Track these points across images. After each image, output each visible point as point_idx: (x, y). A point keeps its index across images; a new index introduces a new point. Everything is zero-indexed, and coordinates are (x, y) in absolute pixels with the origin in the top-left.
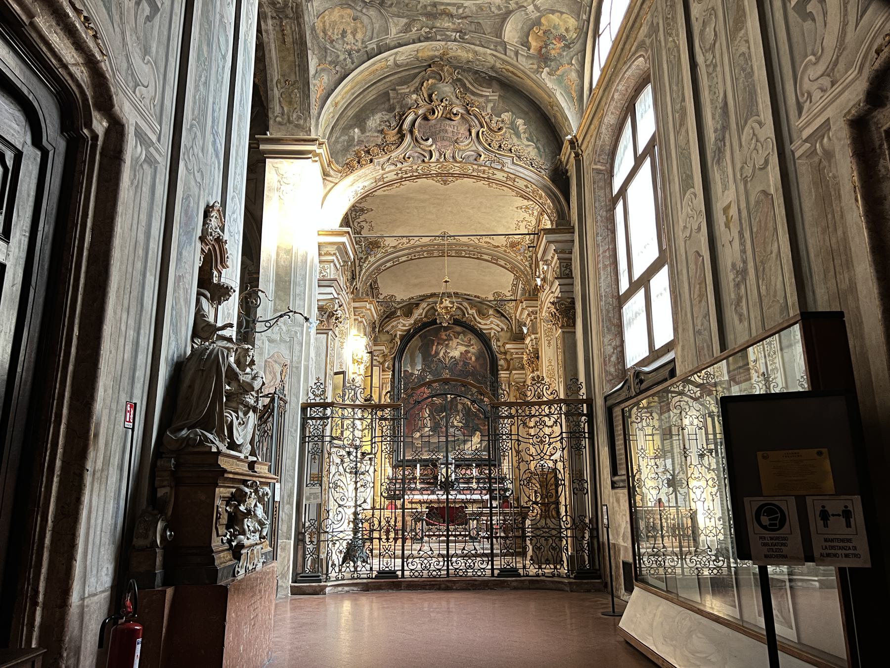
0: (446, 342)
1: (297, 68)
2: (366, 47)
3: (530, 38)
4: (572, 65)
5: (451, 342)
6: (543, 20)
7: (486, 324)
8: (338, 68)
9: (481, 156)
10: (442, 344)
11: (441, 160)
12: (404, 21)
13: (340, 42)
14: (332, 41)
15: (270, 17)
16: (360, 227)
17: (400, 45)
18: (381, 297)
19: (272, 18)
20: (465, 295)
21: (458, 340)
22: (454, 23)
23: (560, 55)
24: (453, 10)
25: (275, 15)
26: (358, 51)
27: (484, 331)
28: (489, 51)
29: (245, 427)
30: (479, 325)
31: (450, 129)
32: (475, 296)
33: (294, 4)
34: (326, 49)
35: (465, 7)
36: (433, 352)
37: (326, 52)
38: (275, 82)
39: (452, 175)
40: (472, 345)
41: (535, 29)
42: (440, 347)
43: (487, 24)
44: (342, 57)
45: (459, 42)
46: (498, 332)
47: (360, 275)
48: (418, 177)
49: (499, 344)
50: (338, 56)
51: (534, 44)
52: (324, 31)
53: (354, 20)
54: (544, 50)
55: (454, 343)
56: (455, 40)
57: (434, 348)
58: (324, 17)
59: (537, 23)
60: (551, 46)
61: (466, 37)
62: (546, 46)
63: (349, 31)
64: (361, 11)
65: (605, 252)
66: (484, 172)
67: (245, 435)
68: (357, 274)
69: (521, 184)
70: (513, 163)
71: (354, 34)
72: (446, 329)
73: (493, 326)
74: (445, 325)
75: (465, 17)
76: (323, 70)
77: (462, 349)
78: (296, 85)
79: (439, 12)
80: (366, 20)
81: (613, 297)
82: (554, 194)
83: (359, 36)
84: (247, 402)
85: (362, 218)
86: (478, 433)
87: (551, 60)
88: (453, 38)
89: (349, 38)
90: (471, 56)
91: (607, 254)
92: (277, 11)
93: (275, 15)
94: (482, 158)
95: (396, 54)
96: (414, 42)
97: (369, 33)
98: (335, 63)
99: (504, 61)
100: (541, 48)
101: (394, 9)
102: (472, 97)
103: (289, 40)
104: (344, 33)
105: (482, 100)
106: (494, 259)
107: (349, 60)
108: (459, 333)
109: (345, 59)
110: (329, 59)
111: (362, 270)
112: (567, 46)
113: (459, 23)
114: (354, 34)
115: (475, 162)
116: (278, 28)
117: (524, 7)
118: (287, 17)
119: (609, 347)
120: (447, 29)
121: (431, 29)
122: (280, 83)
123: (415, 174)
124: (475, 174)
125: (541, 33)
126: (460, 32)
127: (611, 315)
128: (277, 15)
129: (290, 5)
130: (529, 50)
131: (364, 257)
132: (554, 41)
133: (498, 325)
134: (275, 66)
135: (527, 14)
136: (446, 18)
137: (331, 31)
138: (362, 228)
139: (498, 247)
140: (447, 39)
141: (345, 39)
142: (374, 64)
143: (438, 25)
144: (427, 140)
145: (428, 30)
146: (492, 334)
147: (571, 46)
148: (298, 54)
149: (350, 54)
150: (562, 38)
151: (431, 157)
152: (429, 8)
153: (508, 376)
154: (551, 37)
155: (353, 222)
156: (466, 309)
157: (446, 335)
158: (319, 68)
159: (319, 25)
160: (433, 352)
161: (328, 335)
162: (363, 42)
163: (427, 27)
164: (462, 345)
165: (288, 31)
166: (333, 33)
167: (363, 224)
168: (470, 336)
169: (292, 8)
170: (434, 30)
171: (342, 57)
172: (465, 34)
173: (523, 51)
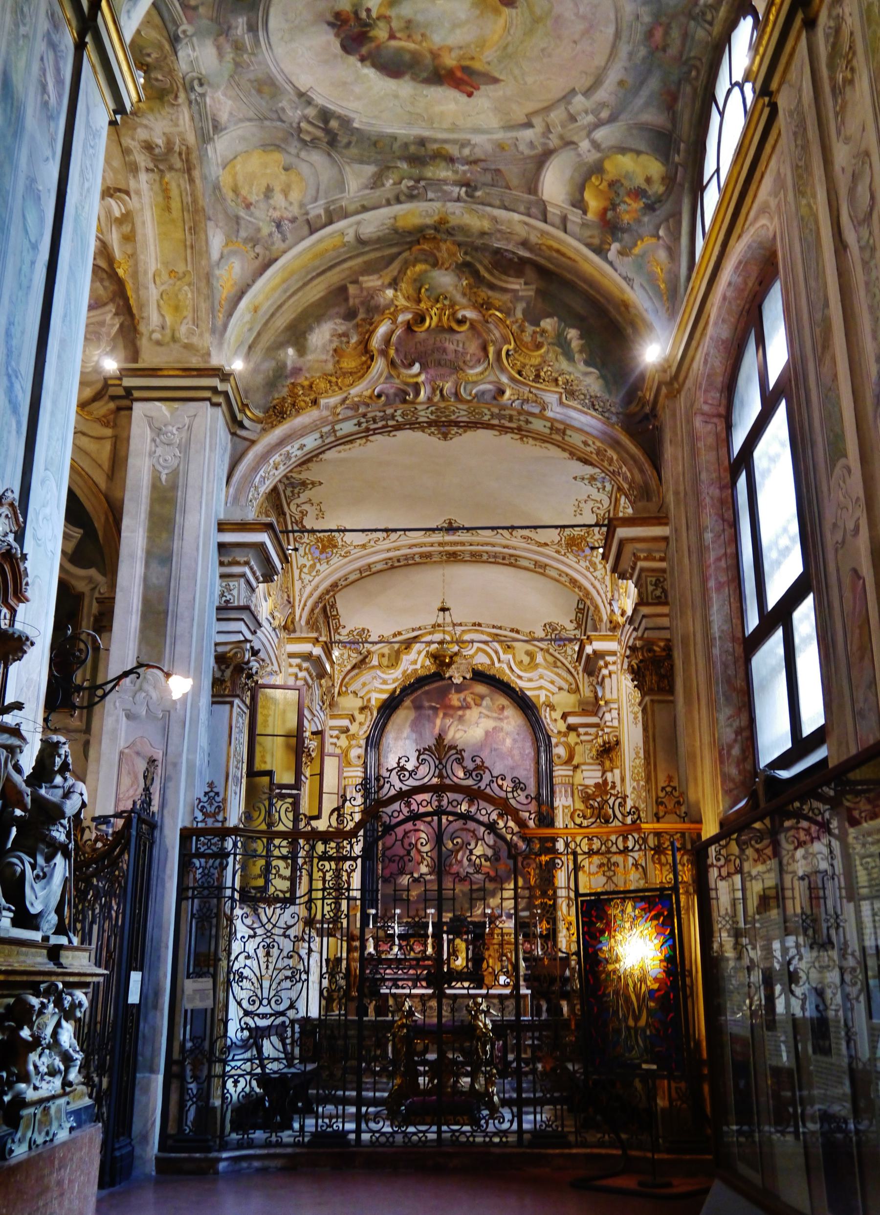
0: (460, 713)
1: (189, 251)
2: (307, 213)
3: (587, 195)
4: (659, 238)
5: (468, 712)
6: (608, 165)
7: (530, 680)
8: (258, 249)
9: (503, 392)
10: (452, 716)
11: (437, 398)
12: (370, 170)
13: (262, 205)
14: (248, 206)
15: (143, 169)
16: (301, 512)
17: (365, 209)
18: (344, 632)
19: (147, 170)
21: (480, 709)
22: (456, 172)
23: (639, 221)
24: (453, 150)
25: (151, 166)
26: (293, 220)
27: (528, 693)
28: (516, 217)
29: (49, 883)
30: (519, 682)
31: (451, 347)
32: (512, 630)
33: (184, 148)
34: (237, 219)
35: (474, 146)
37: (238, 223)
38: (150, 275)
39: (457, 424)
41: (593, 179)
42: (448, 721)
43: (513, 173)
44: (265, 231)
45: (465, 202)
46: (553, 694)
47: (301, 595)
48: (399, 427)
50: (259, 230)
51: (593, 203)
52: (235, 191)
53: (286, 169)
54: (610, 214)
55: (472, 714)
56: (458, 199)
58: (234, 167)
59: (598, 169)
60: (623, 207)
61: (478, 194)
62: (614, 206)
63: (277, 189)
64: (298, 156)
65: (719, 559)
66: (511, 419)
67: (47, 897)
68: (297, 593)
69: (576, 439)
70: (561, 403)
71: (286, 193)
72: (459, 688)
73: (543, 682)
75: (475, 162)
76: (234, 253)
78: (186, 279)
79: (430, 153)
80: (305, 169)
81: (734, 639)
82: (633, 457)
83: (295, 195)
84: (54, 838)
85: (304, 497)
87: (623, 231)
88: (455, 195)
89: (278, 199)
90: (486, 225)
91: (723, 564)
92: (156, 159)
93: (151, 166)
94: (508, 393)
95: (359, 223)
96: (389, 203)
97: (312, 192)
98: (254, 241)
99: (543, 233)
100: (605, 211)
101: (354, 151)
103: (175, 205)
104: (268, 192)
106: (540, 567)
107: (277, 236)
108: (482, 697)
109: (271, 235)
110: (243, 234)
111: (304, 587)
112: (650, 208)
113: (465, 172)
114: (286, 193)
115: (495, 402)
116: (156, 187)
117: (573, 143)
118: (171, 168)
119: (728, 730)
120: (445, 181)
121: (418, 181)
122: (160, 276)
123: (391, 423)
124: (495, 422)
125: (604, 186)
126: (467, 184)
127: (731, 672)
128: (156, 166)
129: (177, 149)
130: (585, 212)
131: (308, 564)
132: (627, 200)
133: (552, 682)
134: (152, 248)
135: (579, 155)
136: (443, 164)
137: (247, 188)
138: (304, 514)
139: (546, 544)
140: (447, 198)
141: (271, 202)
142: (320, 241)
143: (429, 174)
144: (411, 365)
145: (411, 183)
146: (542, 699)
147: (656, 206)
148: (190, 229)
149: (279, 226)
150: (638, 193)
151: (417, 394)
152: (412, 149)
153: (571, 773)
154: (622, 192)
155: (288, 505)
156: (496, 652)
157: (459, 700)
158: (225, 251)
159: (225, 179)
161: (232, 706)
162: (302, 205)
163: (410, 178)
164: (488, 717)
165: (174, 193)
166: (250, 193)
167: (306, 507)
169: (180, 154)
170: (422, 183)
171: (265, 231)
172: (476, 189)
173: (575, 216)
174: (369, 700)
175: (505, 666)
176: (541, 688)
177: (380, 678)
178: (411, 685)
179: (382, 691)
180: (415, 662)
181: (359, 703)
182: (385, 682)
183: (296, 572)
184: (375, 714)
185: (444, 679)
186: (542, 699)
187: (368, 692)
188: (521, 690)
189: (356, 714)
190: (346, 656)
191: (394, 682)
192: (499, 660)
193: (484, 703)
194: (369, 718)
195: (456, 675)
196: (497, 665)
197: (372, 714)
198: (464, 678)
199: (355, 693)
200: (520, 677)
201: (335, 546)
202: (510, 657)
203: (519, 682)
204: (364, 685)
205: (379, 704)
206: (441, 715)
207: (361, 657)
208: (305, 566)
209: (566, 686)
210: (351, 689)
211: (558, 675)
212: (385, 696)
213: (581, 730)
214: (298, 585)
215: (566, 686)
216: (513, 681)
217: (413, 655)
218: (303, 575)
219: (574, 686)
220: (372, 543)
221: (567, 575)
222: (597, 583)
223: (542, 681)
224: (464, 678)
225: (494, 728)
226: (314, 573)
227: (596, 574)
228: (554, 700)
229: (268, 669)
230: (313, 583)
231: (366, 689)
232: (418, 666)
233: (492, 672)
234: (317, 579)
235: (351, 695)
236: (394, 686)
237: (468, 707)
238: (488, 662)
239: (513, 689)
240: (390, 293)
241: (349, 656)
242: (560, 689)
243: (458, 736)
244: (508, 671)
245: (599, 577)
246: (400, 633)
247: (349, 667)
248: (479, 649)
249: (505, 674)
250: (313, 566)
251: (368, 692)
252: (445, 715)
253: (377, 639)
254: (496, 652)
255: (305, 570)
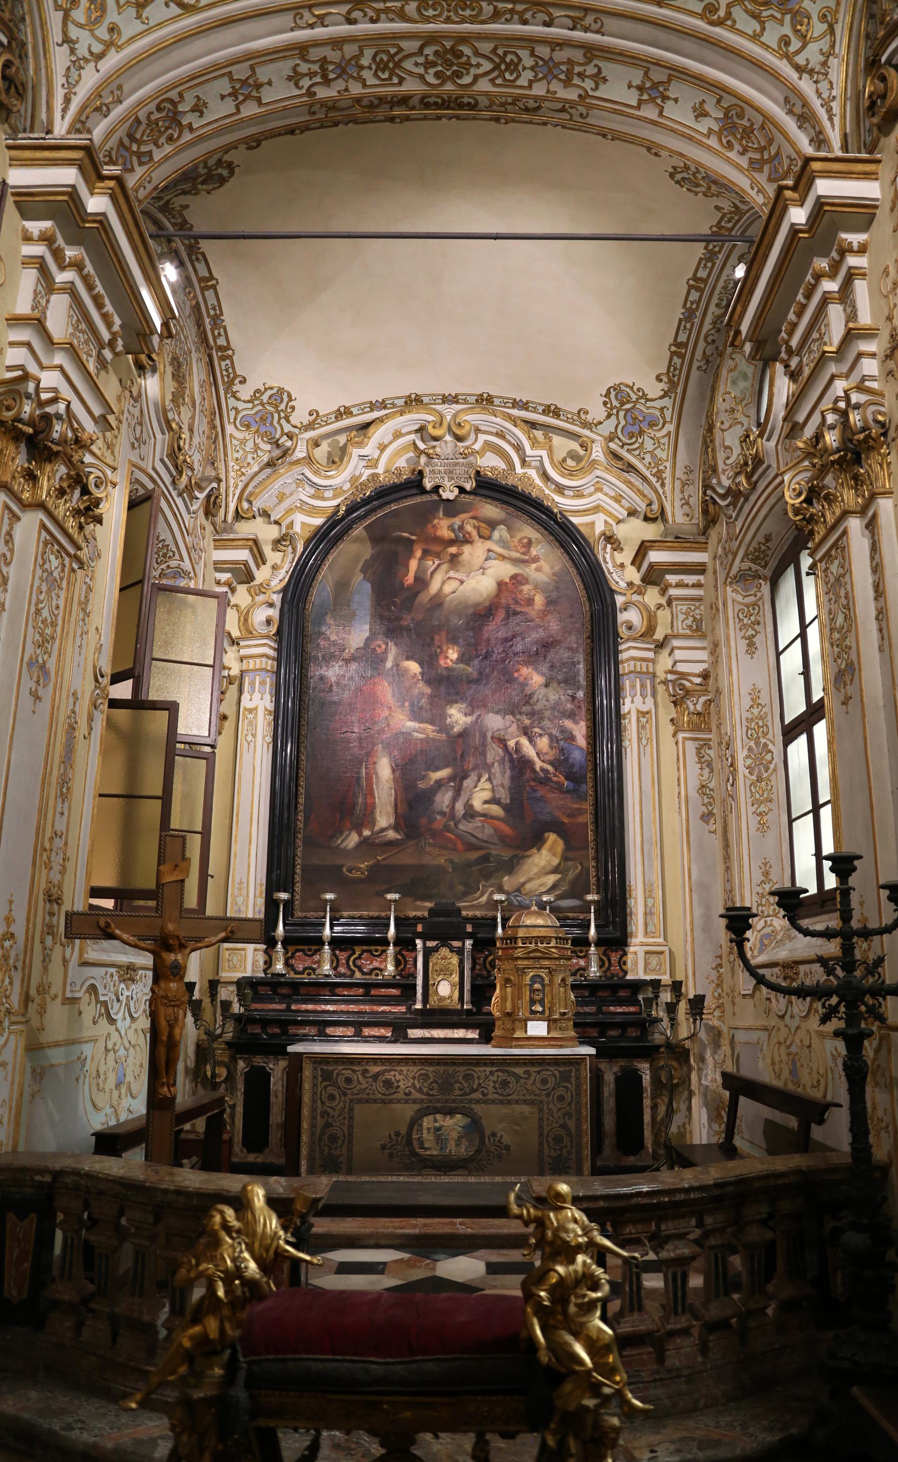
0: (453, 550)
5: (467, 549)
10: (438, 555)
18: (245, 392)
20: (515, 404)
21: (489, 544)
27: (575, 520)
32: (547, 411)
36: (410, 579)
40: (536, 560)
42: (431, 564)
49: (620, 558)
55: (474, 553)
57: (413, 564)
72: (451, 508)
74: (449, 493)
77: (505, 570)
86: (552, 837)
108: (493, 525)
156: (519, 448)
157: (451, 528)
160: (410, 579)
164: (503, 558)
168: (529, 531)
185: (423, 491)
192: (524, 463)
193: (496, 535)
195: (447, 484)
196: (519, 470)
198: (462, 490)
204: (281, 497)
206: (418, 554)
224: (462, 490)
225: (514, 577)
237: (468, 541)
239: (548, 512)
243: (448, 589)
252: (426, 553)
253: (306, 419)
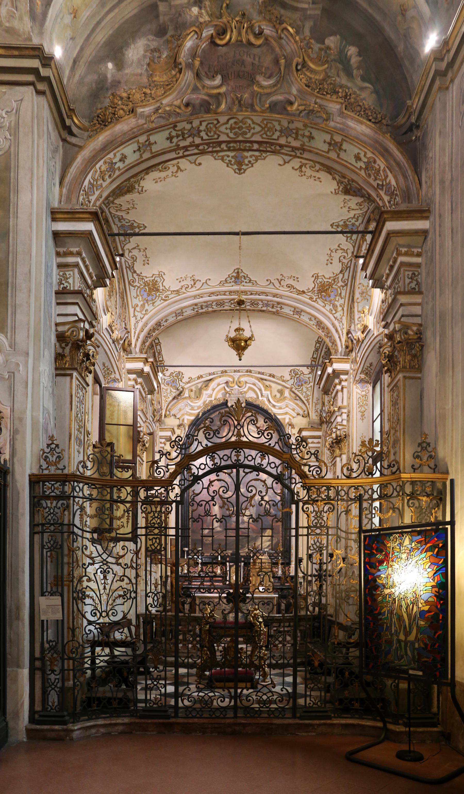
31: (249, 60)
102: (282, 11)
105: (297, 15)
144: (213, 78)
174: (183, 420)
175: (265, 399)
176: (286, 413)
177: (190, 405)
178: (209, 411)
179: (190, 414)
180: (210, 396)
181: (177, 422)
182: (192, 409)
183: (132, 310)
184: (187, 429)
186: (287, 421)
187: (183, 415)
188: (274, 415)
189: (176, 429)
190: (169, 391)
191: (198, 409)
194: (183, 432)
197: (185, 429)
199: (175, 416)
200: (274, 406)
201: (158, 290)
202: (269, 393)
203: (273, 409)
205: (189, 423)
207: (178, 392)
208: (137, 306)
209: (301, 412)
210: (172, 412)
211: (297, 404)
212: (192, 418)
213: (310, 440)
214: (133, 320)
215: (301, 412)
216: (270, 409)
217: (209, 391)
218: (136, 313)
219: (306, 413)
220: (183, 290)
221: (316, 318)
222: (336, 323)
223: (287, 409)
226: (144, 312)
227: (338, 315)
228: (294, 421)
229: (112, 376)
230: (144, 320)
231: (182, 413)
232: (213, 399)
233: (257, 403)
234: (146, 317)
235: (172, 417)
236: (198, 411)
238: (255, 396)
240: (195, 10)
241: (171, 391)
242: (298, 414)
244: (267, 402)
245: (339, 317)
246: (202, 377)
247: (171, 399)
248: (250, 388)
249: (265, 404)
250: (143, 306)
251: (183, 415)
254: (260, 390)
255: (138, 309)
